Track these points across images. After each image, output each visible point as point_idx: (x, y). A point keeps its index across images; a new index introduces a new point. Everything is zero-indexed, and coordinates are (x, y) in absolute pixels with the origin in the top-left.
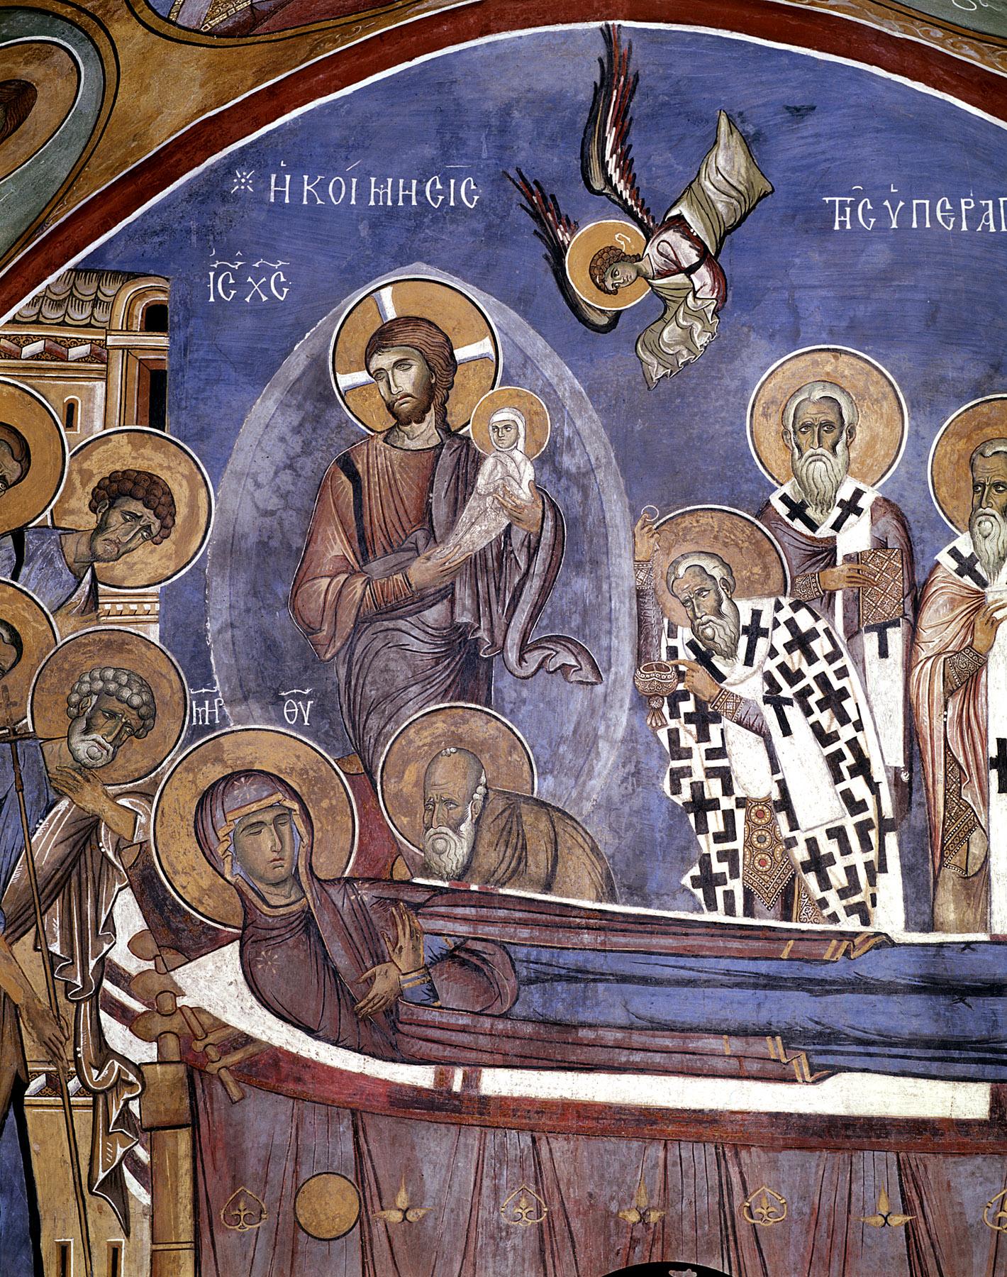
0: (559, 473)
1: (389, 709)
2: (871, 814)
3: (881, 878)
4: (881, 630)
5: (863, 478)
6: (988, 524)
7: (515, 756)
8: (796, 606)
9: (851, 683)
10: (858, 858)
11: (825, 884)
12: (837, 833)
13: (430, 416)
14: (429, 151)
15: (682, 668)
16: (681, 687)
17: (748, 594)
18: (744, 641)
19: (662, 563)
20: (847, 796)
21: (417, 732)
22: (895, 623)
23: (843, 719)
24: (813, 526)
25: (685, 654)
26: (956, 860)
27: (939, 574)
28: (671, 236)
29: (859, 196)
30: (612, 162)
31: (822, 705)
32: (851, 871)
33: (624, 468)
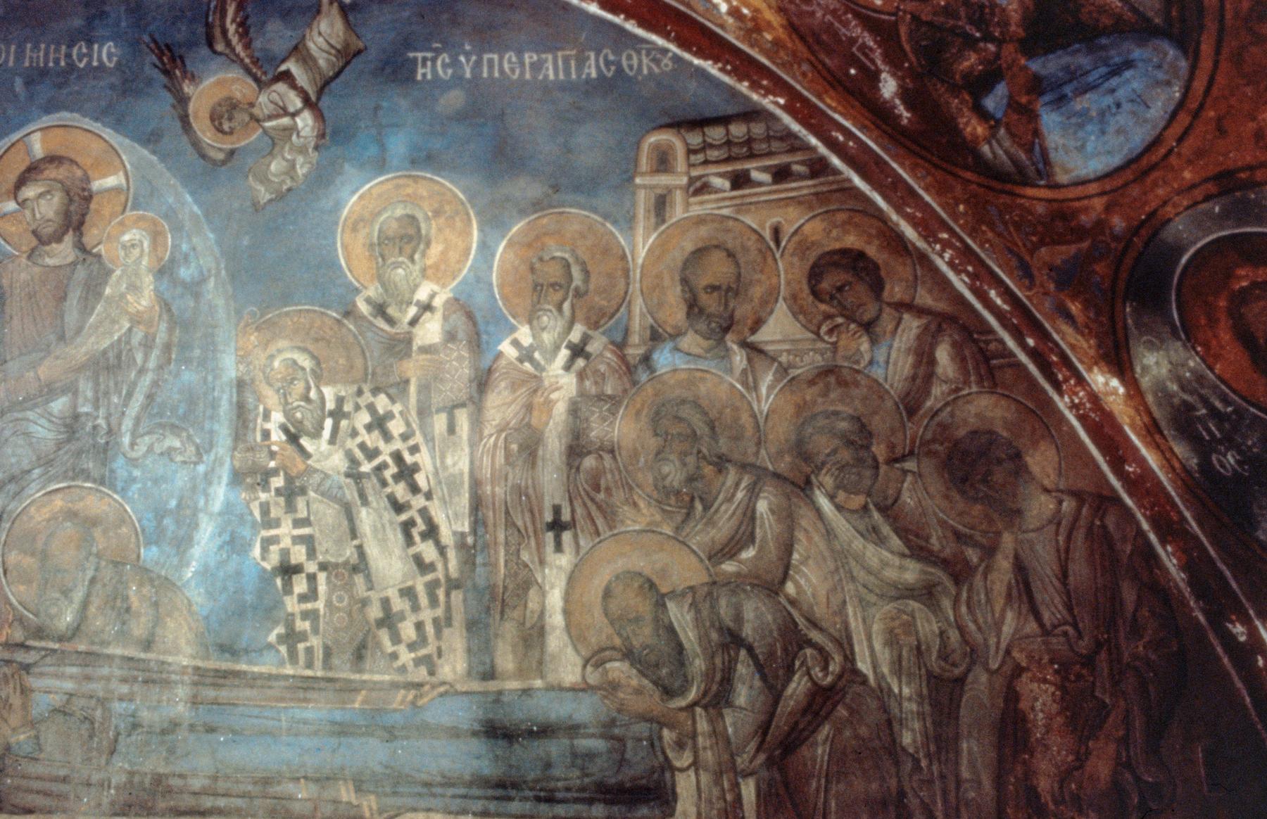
0: (175, 281)
1: (12, 488)
2: (440, 574)
3: (446, 632)
4: (451, 410)
5: (437, 280)
6: (545, 318)
7: (124, 530)
8: (376, 391)
9: (424, 458)
10: (427, 615)
11: (396, 639)
12: (408, 593)
13: (69, 238)
14: (78, 22)
15: (275, 448)
16: (272, 464)
17: (332, 382)
18: (329, 423)
19: (260, 358)
20: (418, 560)
21: (38, 510)
22: (463, 405)
23: (415, 489)
24: (391, 321)
25: (277, 436)
26: (516, 614)
27: (503, 362)
28: (281, 87)
29: (437, 51)
30: (231, 28)
31: (397, 478)
32: (419, 626)
33: (233, 277)
